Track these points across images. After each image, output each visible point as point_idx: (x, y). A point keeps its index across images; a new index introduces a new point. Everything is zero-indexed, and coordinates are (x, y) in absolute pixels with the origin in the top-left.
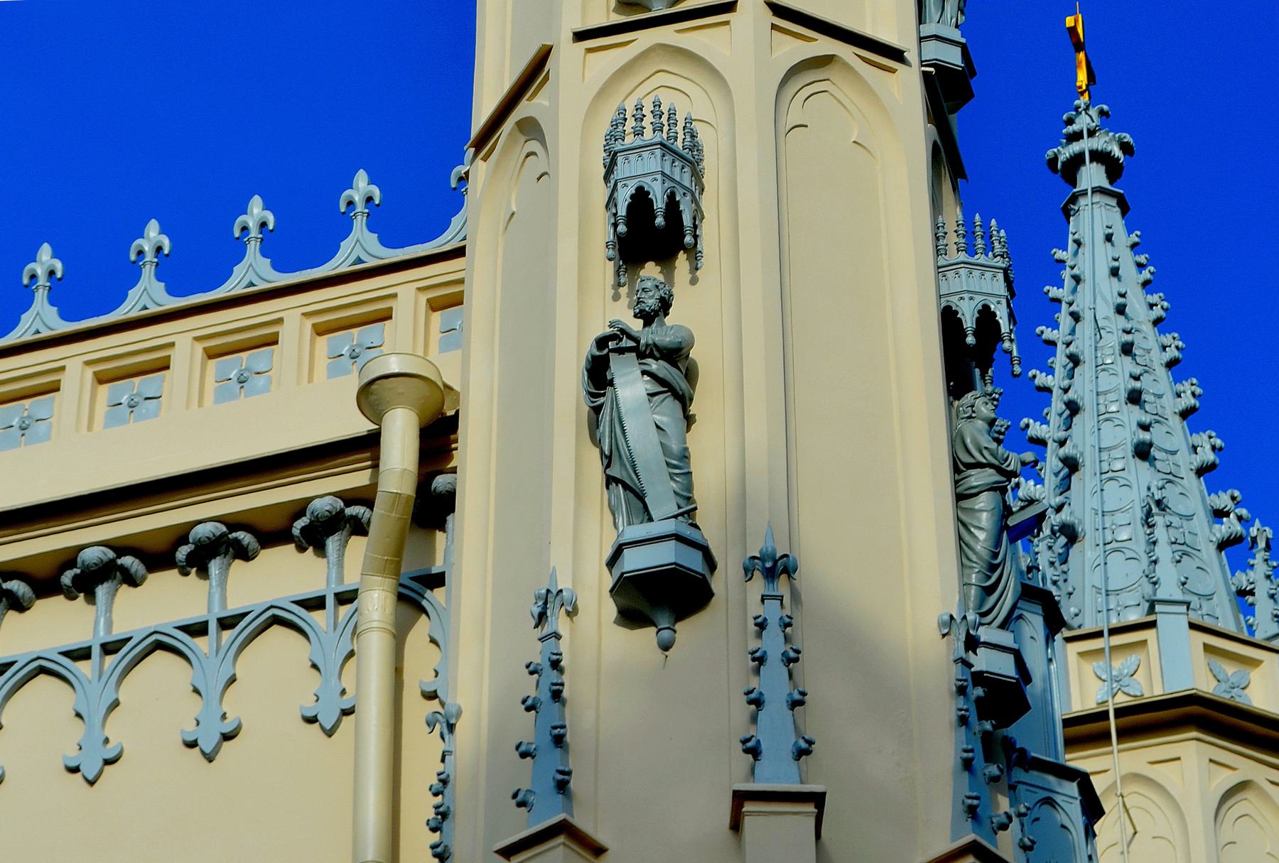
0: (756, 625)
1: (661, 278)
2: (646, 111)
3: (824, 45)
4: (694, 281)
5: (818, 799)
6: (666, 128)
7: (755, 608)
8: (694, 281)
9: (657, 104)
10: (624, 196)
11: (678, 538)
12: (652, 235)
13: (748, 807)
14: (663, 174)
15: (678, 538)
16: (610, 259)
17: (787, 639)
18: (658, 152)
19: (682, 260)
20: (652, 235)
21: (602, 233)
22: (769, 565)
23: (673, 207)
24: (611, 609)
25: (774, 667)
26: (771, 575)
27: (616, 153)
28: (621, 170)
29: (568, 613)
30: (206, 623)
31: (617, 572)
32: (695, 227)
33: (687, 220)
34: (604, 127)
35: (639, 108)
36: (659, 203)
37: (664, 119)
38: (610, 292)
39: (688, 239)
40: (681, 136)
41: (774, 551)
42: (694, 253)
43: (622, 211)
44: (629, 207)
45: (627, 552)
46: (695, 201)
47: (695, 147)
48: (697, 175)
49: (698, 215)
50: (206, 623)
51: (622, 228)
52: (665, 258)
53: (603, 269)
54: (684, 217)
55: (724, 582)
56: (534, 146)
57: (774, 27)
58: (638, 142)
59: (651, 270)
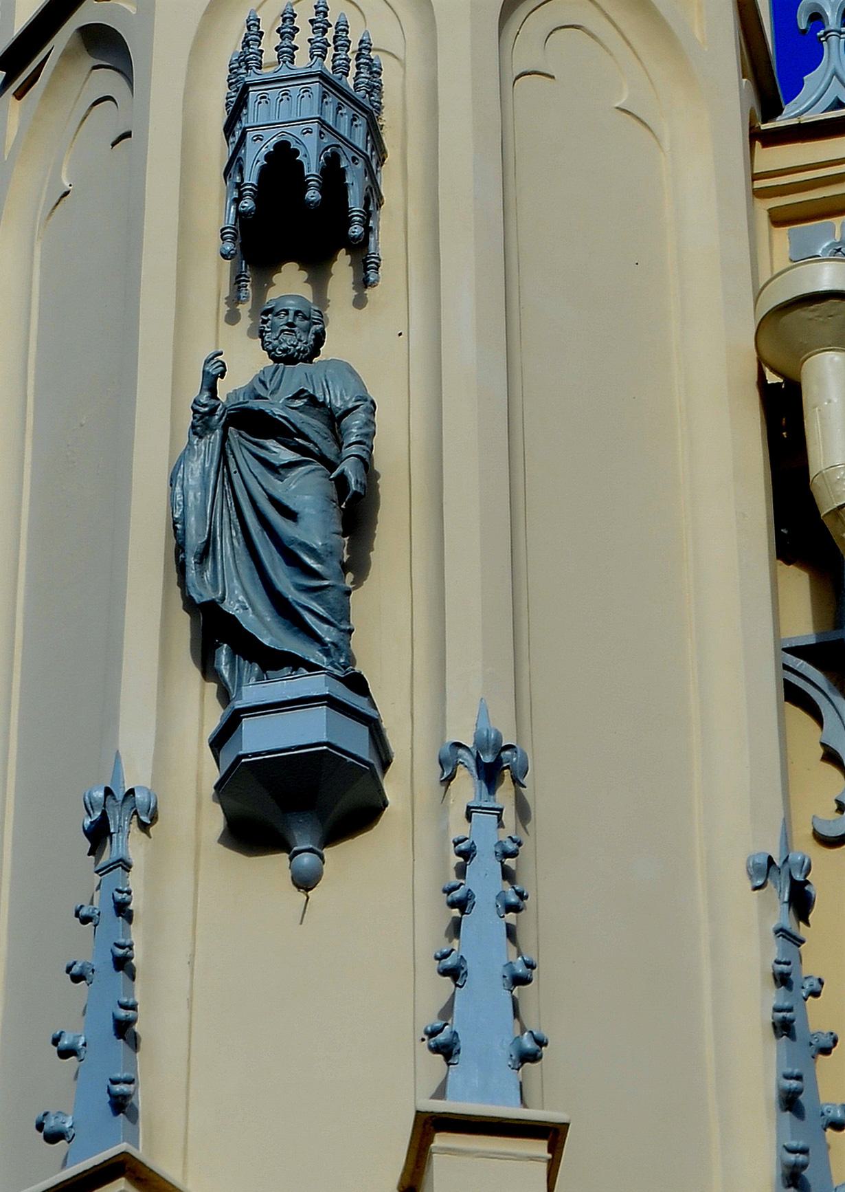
0: (459, 854)
1: (307, 292)
2: (302, 22)
4: (360, 302)
5: (553, 1134)
6: (331, 51)
8: (360, 302)
10: (255, 157)
11: (331, 702)
12: (297, 219)
14: (322, 123)
15: (331, 702)
16: (224, 256)
18: (316, 87)
19: (342, 266)
20: (297, 219)
21: (215, 211)
23: (333, 174)
25: (485, 922)
27: (246, 88)
28: (254, 115)
31: (228, 758)
32: (367, 215)
33: (355, 201)
34: (231, 45)
35: (289, 17)
36: (312, 165)
37: (331, 32)
38: (225, 309)
39: (356, 230)
40: (353, 71)
42: (361, 252)
43: (251, 176)
44: (263, 171)
45: (247, 724)
46: (371, 174)
47: (375, 88)
48: (374, 131)
49: (373, 197)
51: (248, 204)
52: (317, 265)
53: (213, 273)
54: (351, 193)
56: (108, 81)
58: (285, 72)
59: (290, 283)
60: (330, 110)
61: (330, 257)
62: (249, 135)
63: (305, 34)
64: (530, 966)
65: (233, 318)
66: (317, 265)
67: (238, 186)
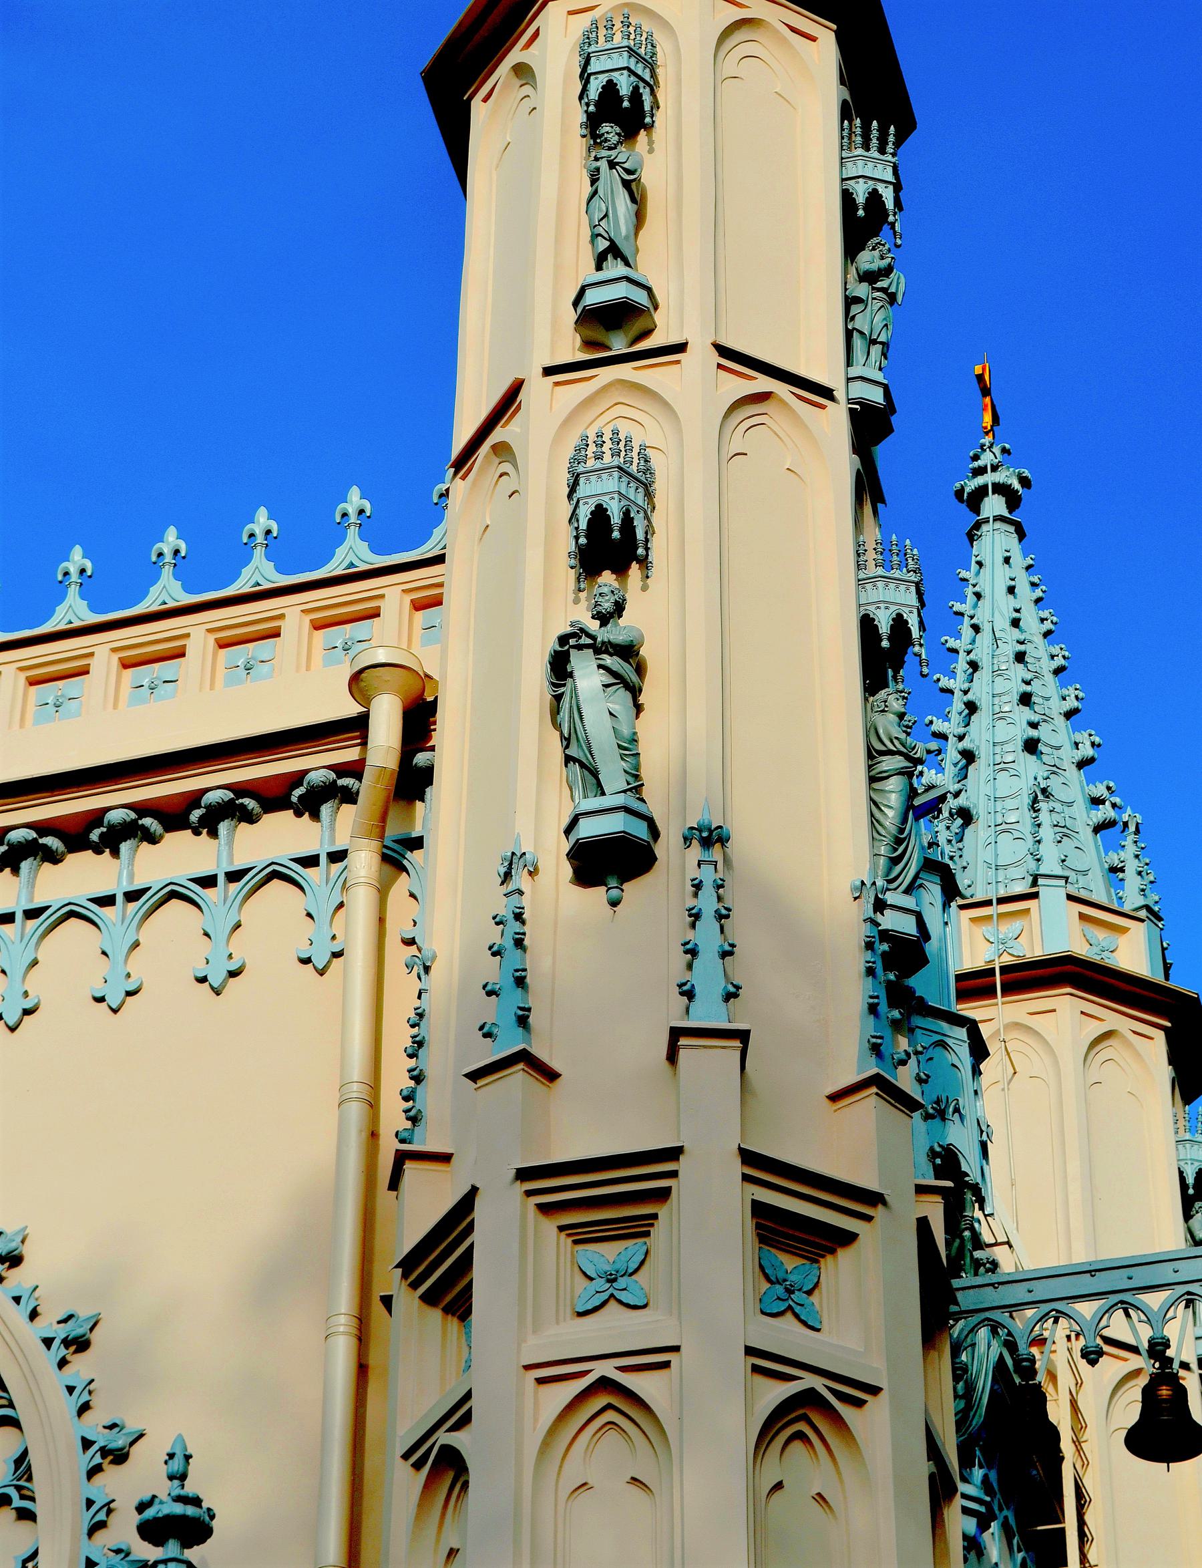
0: (693, 886)
1: (616, 584)
3: (764, 383)
4: (645, 588)
5: (743, 1036)
6: (623, 454)
7: (692, 872)
8: (645, 588)
9: (616, 433)
10: (585, 513)
12: (608, 547)
13: (683, 1041)
16: (572, 568)
17: (720, 899)
18: (616, 475)
20: (608, 547)
21: (566, 544)
22: (705, 834)
23: (627, 523)
24: (567, 870)
25: (708, 923)
26: (707, 843)
27: (578, 475)
28: (583, 490)
29: (530, 873)
30: (318, 856)
31: (573, 838)
32: (647, 540)
33: (640, 535)
36: (616, 519)
37: (622, 444)
38: (571, 596)
39: (641, 551)
40: (636, 461)
41: (710, 822)
42: (644, 562)
43: (583, 525)
45: (582, 822)
46: (647, 517)
47: (648, 470)
48: (649, 495)
49: (649, 530)
50: (318, 856)
51: (583, 541)
52: (621, 570)
53: (566, 574)
55: (668, 848)
56: (506, 467)
57: (720, 366)
58: (598, 465)
59: (607, 578)
60: (624, 485)
61: (628, 567)
62: (581, 502)
63: (608, 445)
64: (733, 946)
65: (576, 601)
66: (621, 570)
67: (577, 529)
